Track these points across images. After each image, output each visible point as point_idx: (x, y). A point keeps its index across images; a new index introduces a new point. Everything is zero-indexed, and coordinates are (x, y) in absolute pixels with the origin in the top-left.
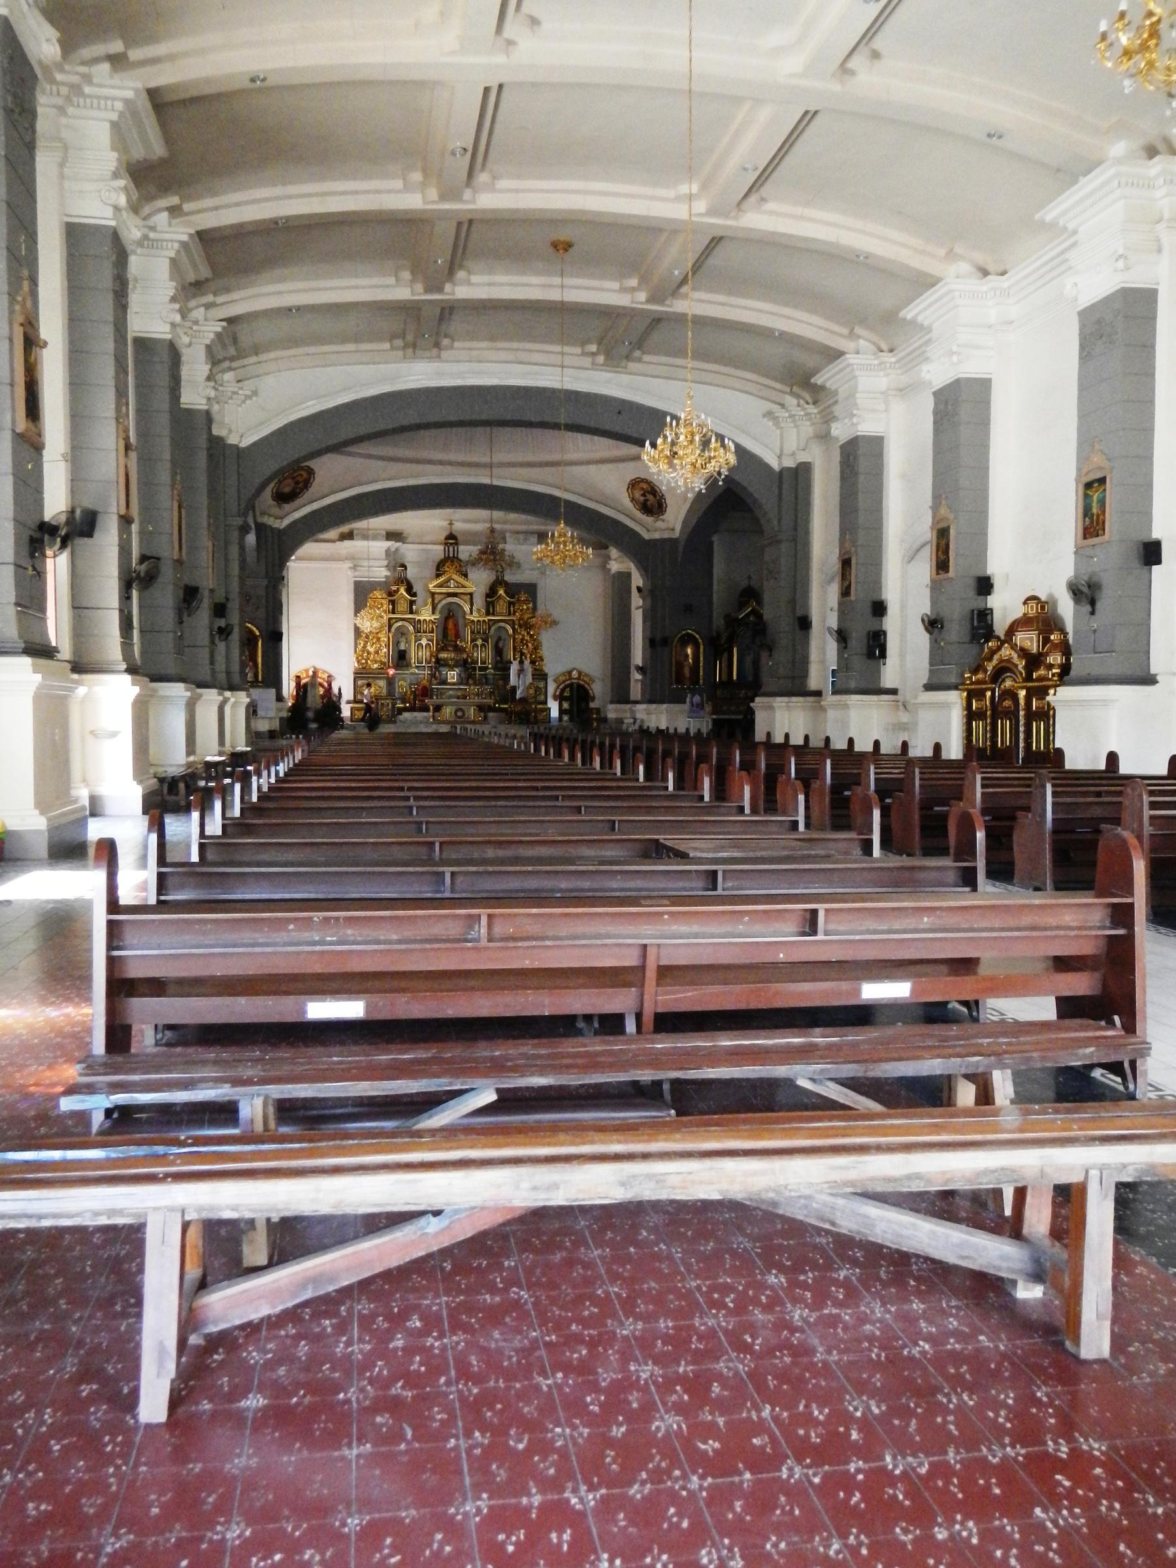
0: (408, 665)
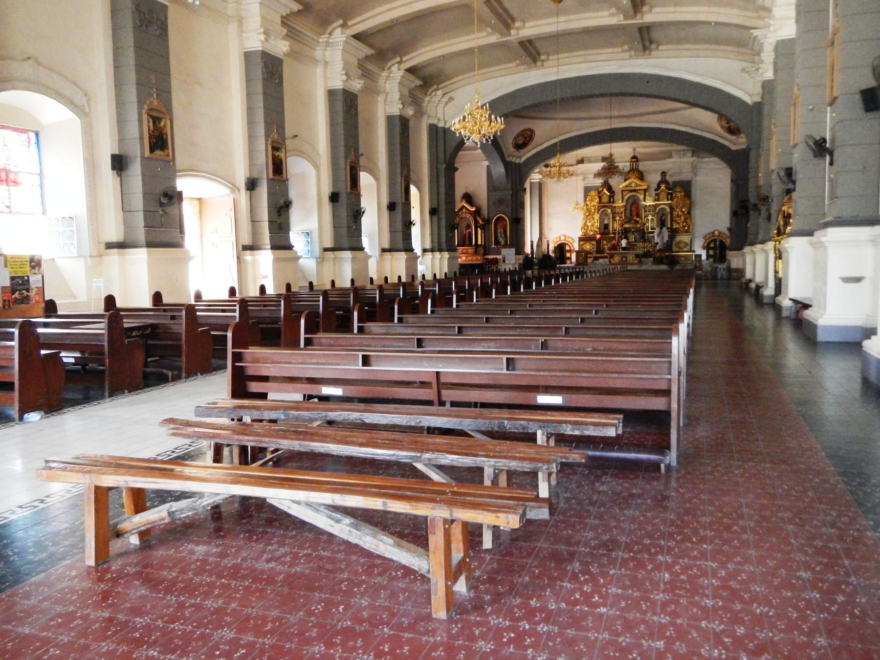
0: (609, 233)
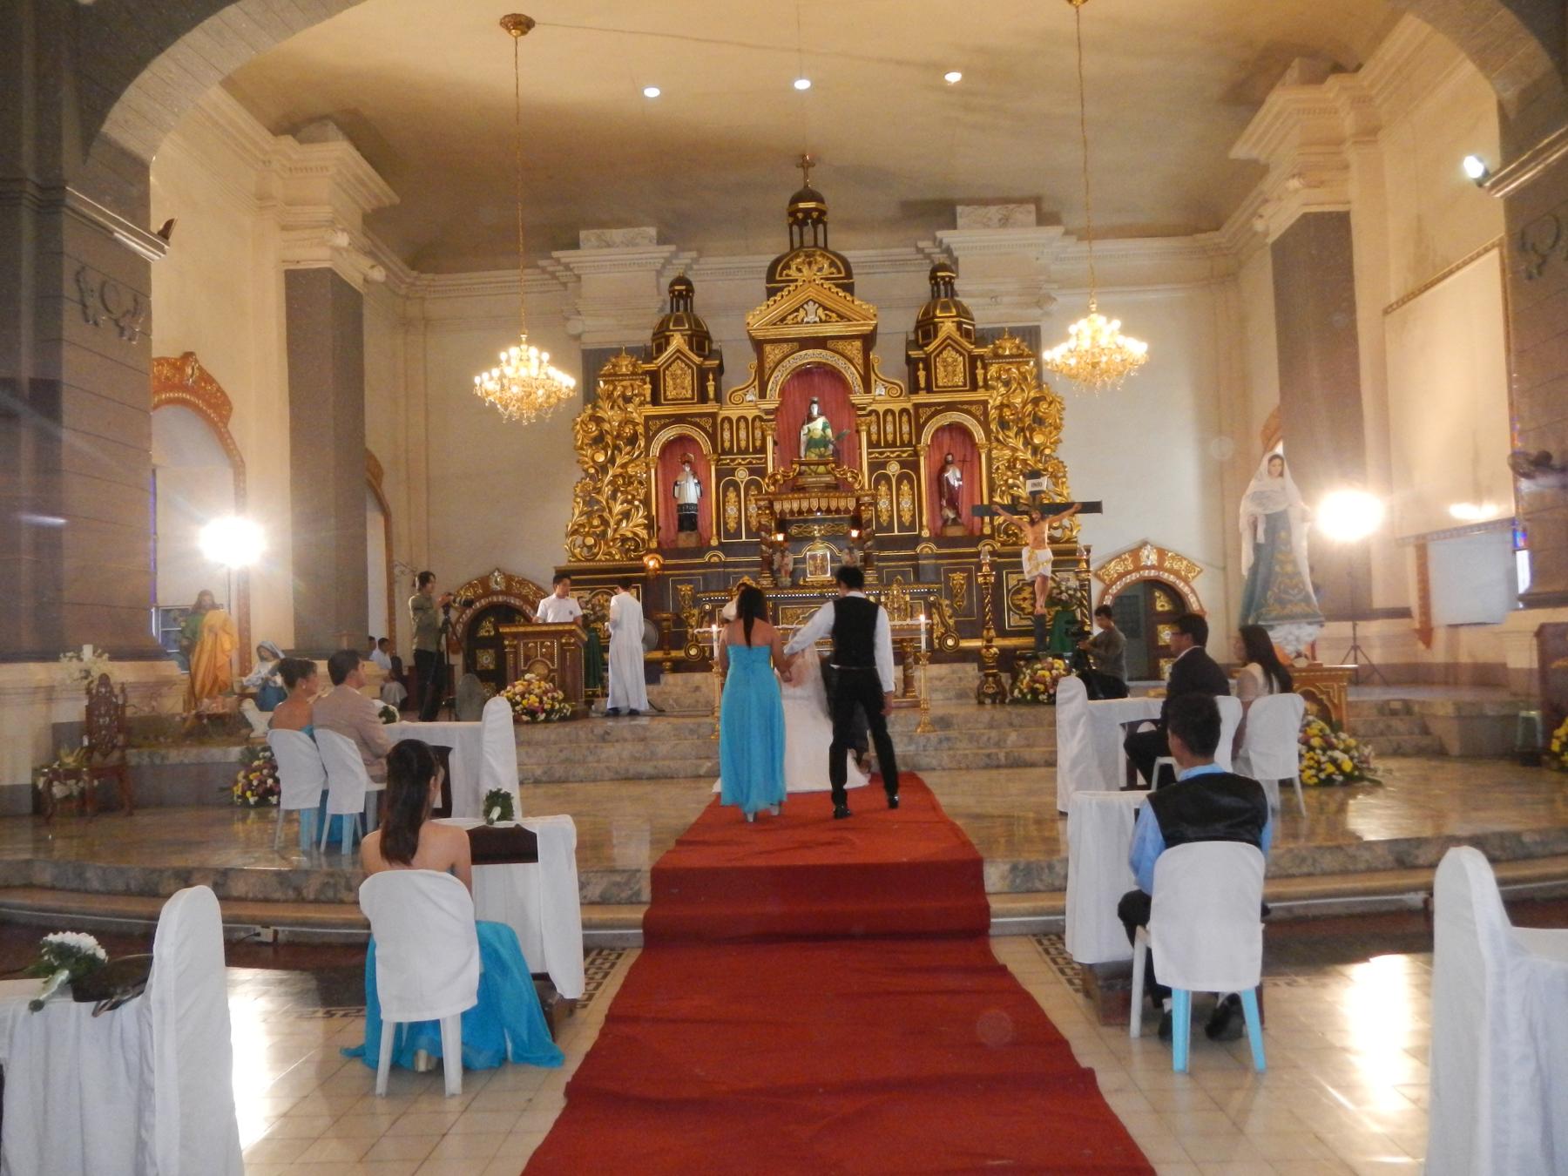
0: (701, 550)
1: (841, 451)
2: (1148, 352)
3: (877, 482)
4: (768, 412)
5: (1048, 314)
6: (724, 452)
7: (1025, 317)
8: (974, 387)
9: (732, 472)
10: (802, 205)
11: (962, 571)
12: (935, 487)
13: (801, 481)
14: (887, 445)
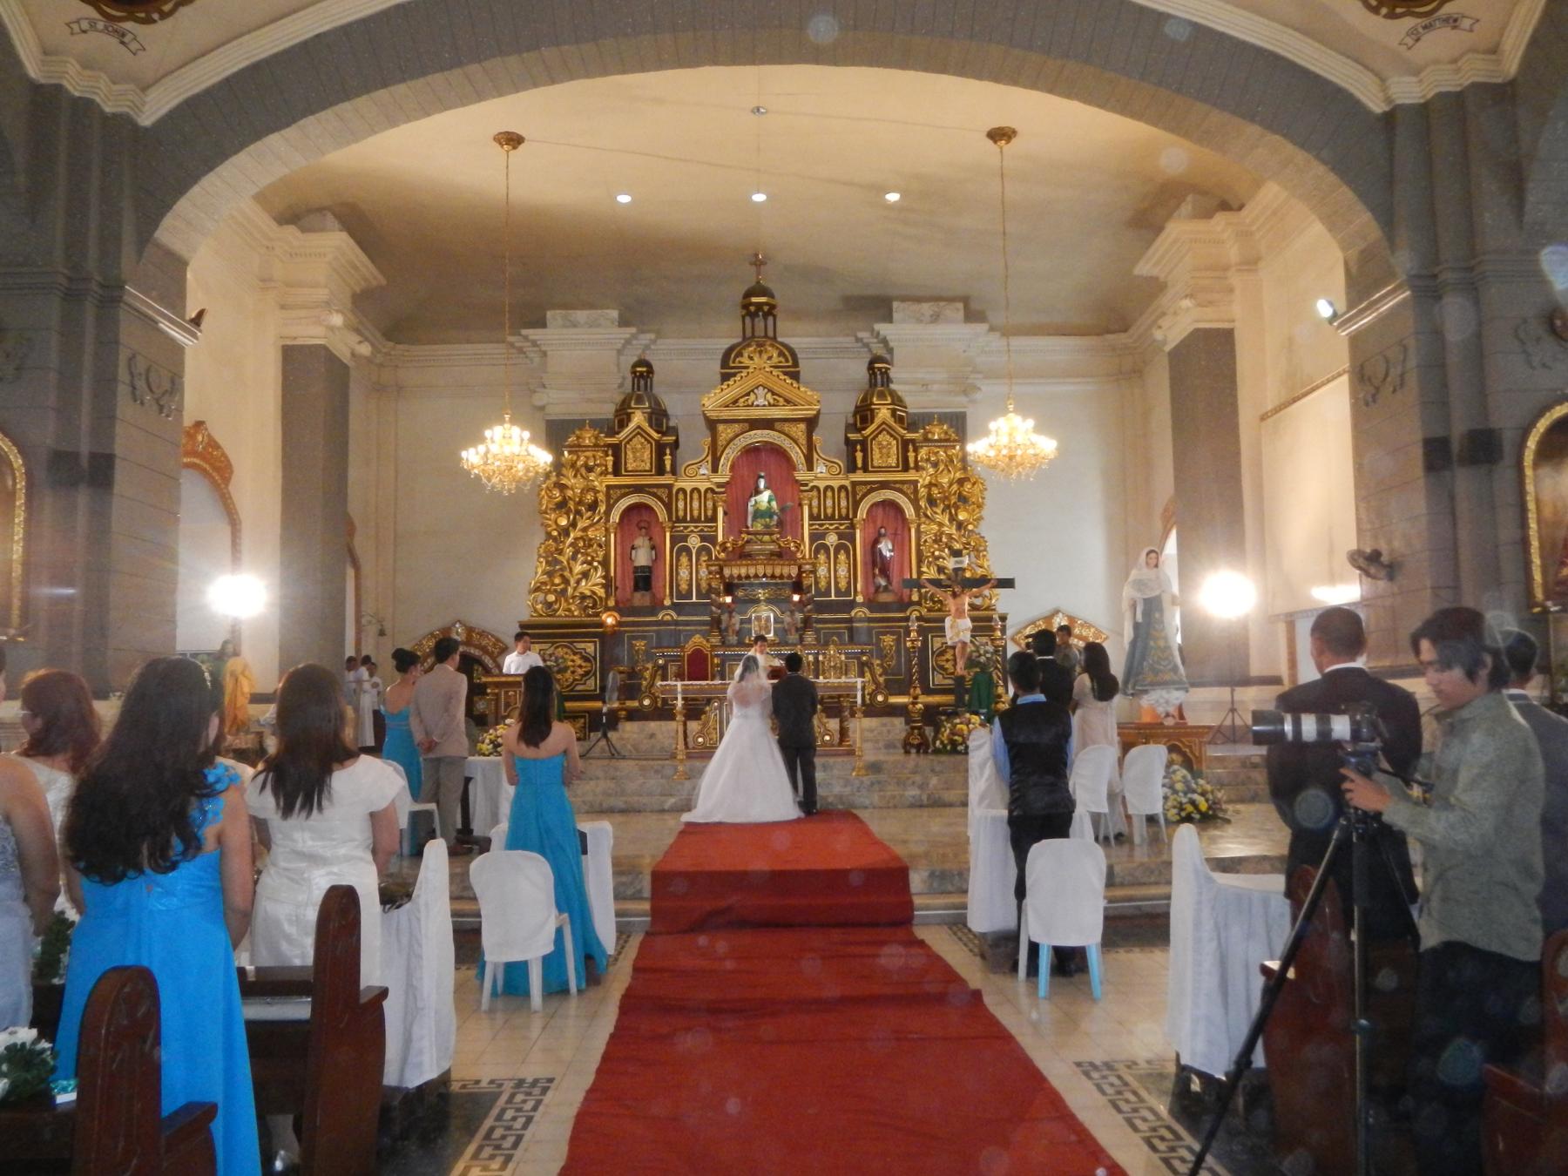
0: (656, 606)
1: (785, 520)
2: (1058, 449)
3: (817, 551)
4: (719, 485)
5: (973, 402)
6: (678, 520)
7: (953, 404)
8: (906, 469)
9: (685, 538)
10: (754, 300)
11: (892, 634)
12: (869, 558)
13: (748, 548)
14: (827, 518)
